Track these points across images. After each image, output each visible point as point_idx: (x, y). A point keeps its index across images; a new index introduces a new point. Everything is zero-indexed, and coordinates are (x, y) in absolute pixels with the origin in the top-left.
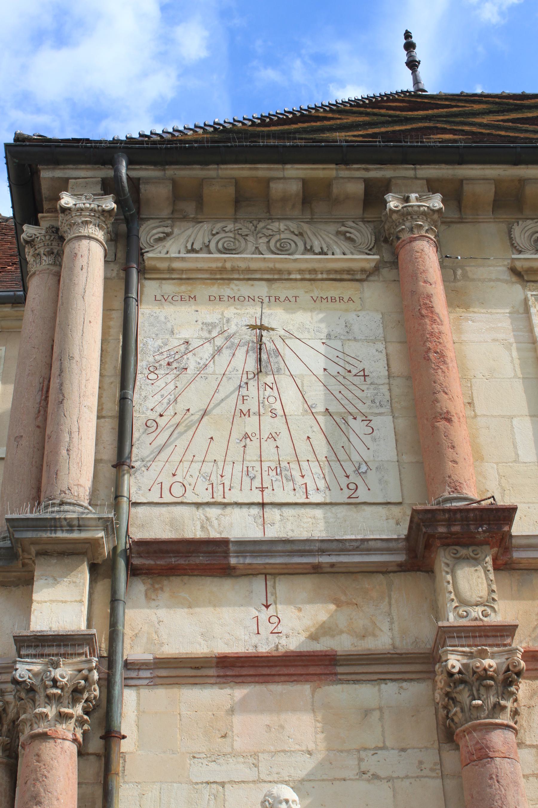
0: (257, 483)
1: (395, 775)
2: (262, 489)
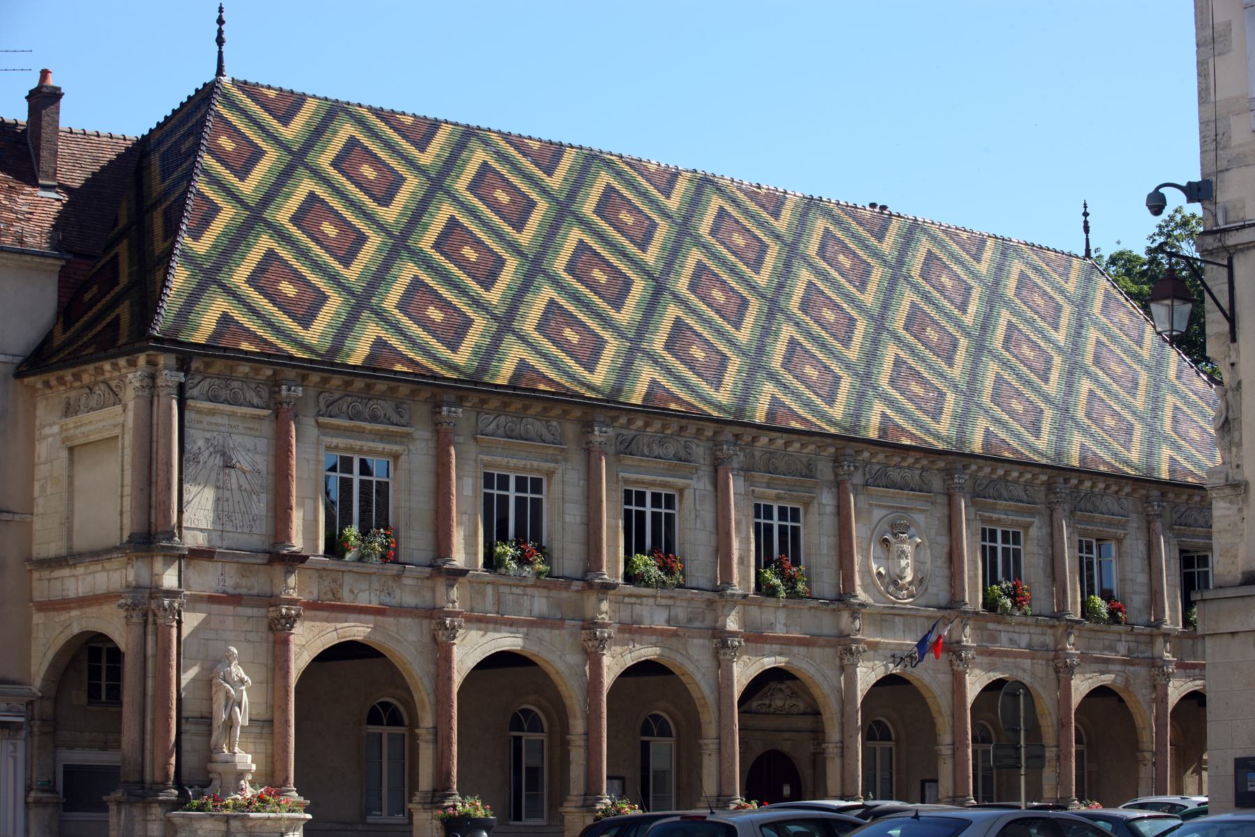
2: (223, 524)
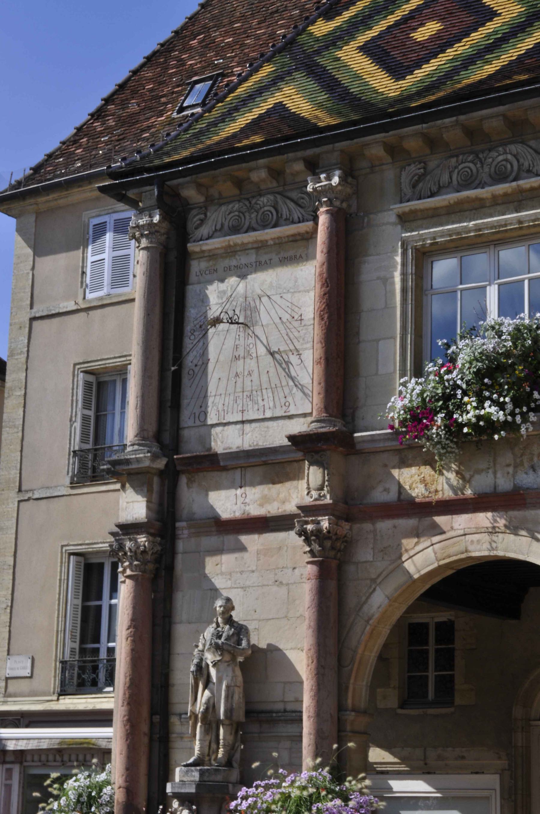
0: (240, 408)
1: (290, 582)
